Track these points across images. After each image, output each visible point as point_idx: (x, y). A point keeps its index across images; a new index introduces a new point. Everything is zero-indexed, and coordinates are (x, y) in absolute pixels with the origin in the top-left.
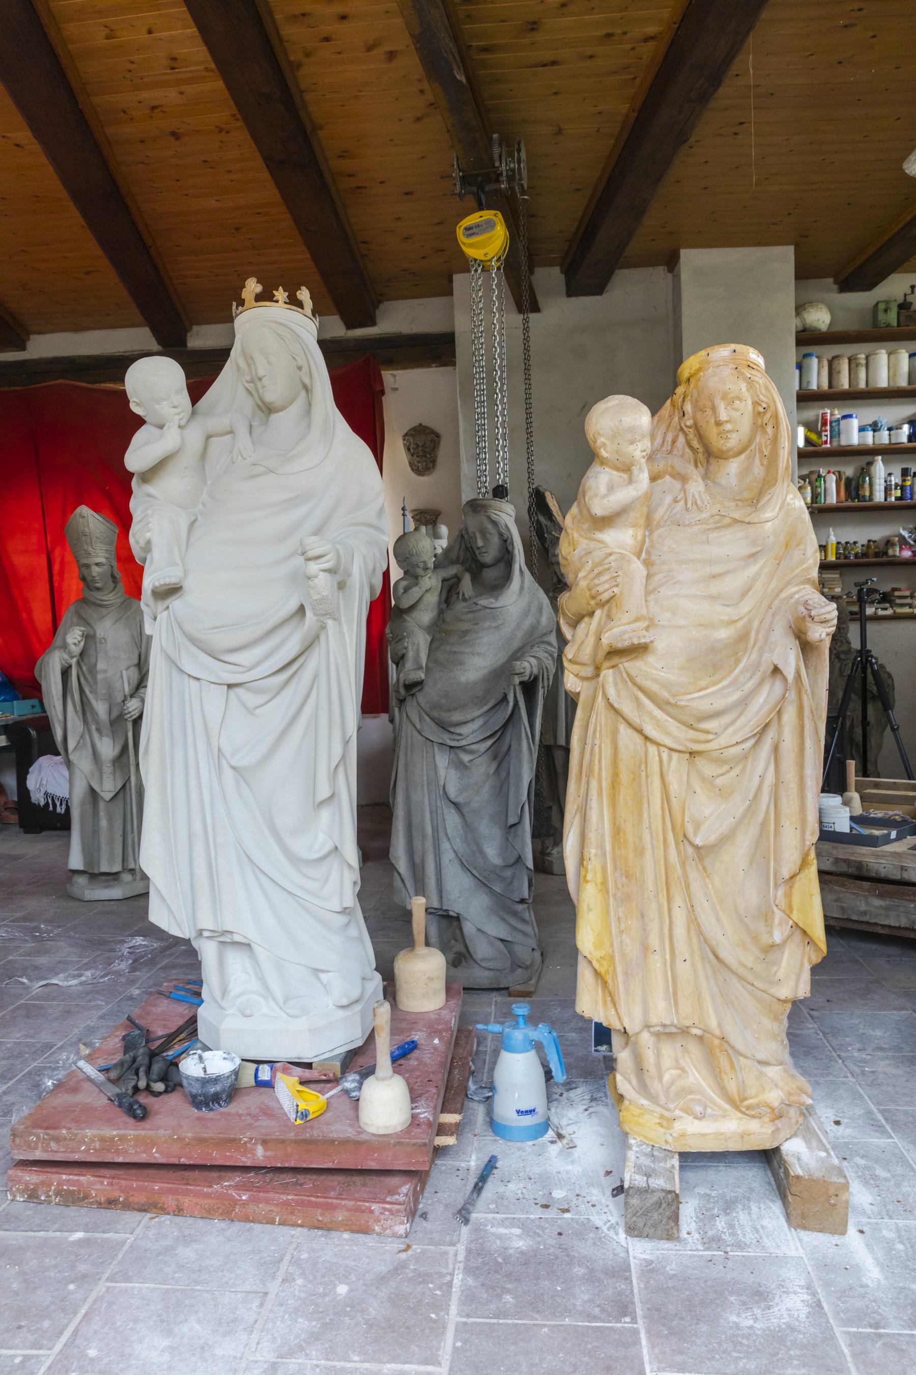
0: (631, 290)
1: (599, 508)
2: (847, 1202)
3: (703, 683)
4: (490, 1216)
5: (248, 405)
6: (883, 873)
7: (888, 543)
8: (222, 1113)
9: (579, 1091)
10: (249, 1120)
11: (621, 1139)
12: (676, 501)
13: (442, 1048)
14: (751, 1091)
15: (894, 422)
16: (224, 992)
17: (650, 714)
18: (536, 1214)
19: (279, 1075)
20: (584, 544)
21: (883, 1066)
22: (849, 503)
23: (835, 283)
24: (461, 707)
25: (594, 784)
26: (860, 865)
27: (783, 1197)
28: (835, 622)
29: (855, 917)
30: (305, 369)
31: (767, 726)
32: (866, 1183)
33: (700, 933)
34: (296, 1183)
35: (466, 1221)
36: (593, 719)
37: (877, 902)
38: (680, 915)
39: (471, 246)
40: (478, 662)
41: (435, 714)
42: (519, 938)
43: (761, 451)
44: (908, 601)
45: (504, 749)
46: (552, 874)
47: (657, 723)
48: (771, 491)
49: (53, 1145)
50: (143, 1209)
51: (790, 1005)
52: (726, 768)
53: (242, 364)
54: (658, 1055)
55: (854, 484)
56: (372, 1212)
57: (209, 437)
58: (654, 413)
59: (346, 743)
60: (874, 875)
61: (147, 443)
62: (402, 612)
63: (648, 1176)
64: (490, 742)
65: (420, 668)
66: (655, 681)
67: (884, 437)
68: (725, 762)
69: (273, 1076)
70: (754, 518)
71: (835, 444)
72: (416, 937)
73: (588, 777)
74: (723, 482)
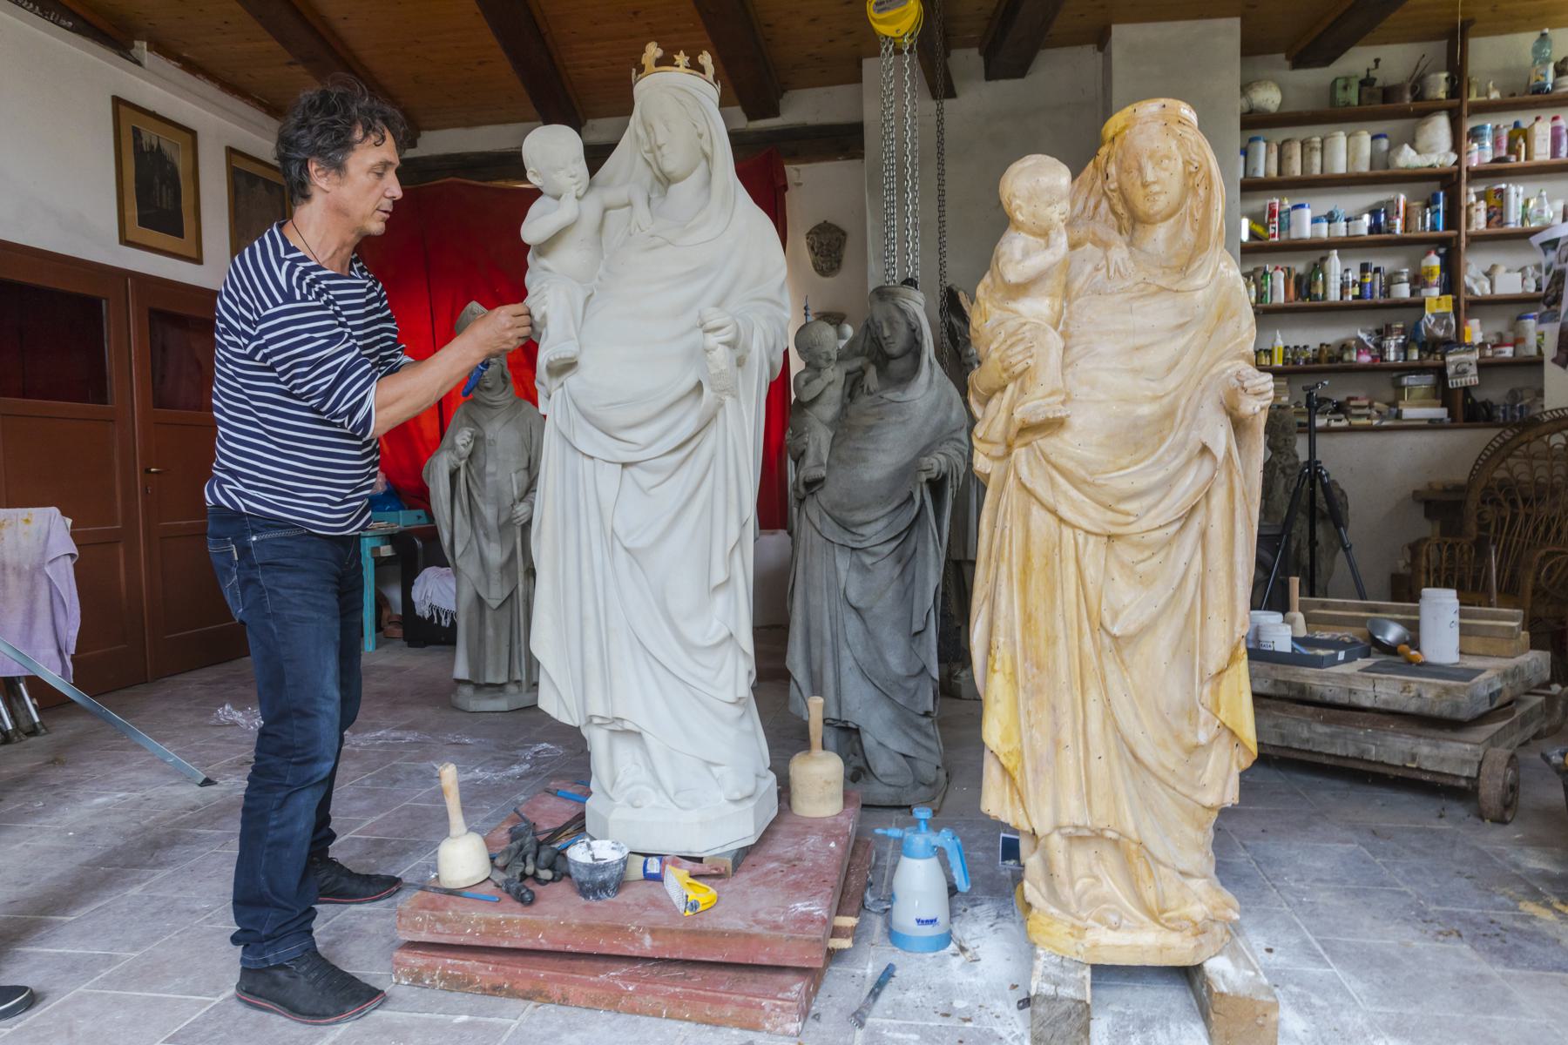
0: (1058, 72)
1: (1013, 274)
2: (1277, 1023)
3: (1124, 462)
4: (887, 1021)
5: (647, 177)
6: (1329, 696)
7: (1344, 347)
8: (610, 903)
9: (984, 907)
10: (637, 910)
11: (1029, 950)
12: (1097, 269)
13: (839, 851)
14: (1172, 904)
15: (1352, 212)
16: (613, 783)
17: (1065, 494)
18: (936, 1021)
19: (668, 867)
20: (996, 315)
21: (1324, 897)
22: (1300, 303)
23: (1287, 58)
24: (865, 507)
25: (1004, 569)
26: (1302, 688)
27: (1205, 1017)
28: (1271, 394)
29: (1296, 745)
30: (706, 136)
31: (1194, 508)
32: (1300, 1010)
33: (1117, 729)
34: (684, 977)
35: (861, 1025)
36: (1004, 500)
37: (1321, 729)
38: (1095, 710)
39: (883, 22)
40: (884, 457)
41: (837, 513)
42: (923, 754)
43: (1192, 215)
44: (1366, 411)
45: (909, 552)
46: (960, 698)
47: (1072, 503)
48: (1203, 256)
49: (439, 926)
50: (527, 997)
51: (1215, 815)
52: (1147, 553)
53: (641, 132)
54: (1070, 860)
55: (1305, 282)
56: (762, 1008)
57: (606, 210)
58: (1075, 175)
59: (743, 525)
60: (1317, 698)
61: (544, 214)
62: (802, 406)
63: (1057, 985)
64: (894, 544)
65: (822, 464)
66: (1072, 459)
67: (1341, 229)
68: (1147, 547)
69: (663, 869)
70: (1183, 286)
71: (1284, 237)
72: (812, 739)
73: (997, 561)
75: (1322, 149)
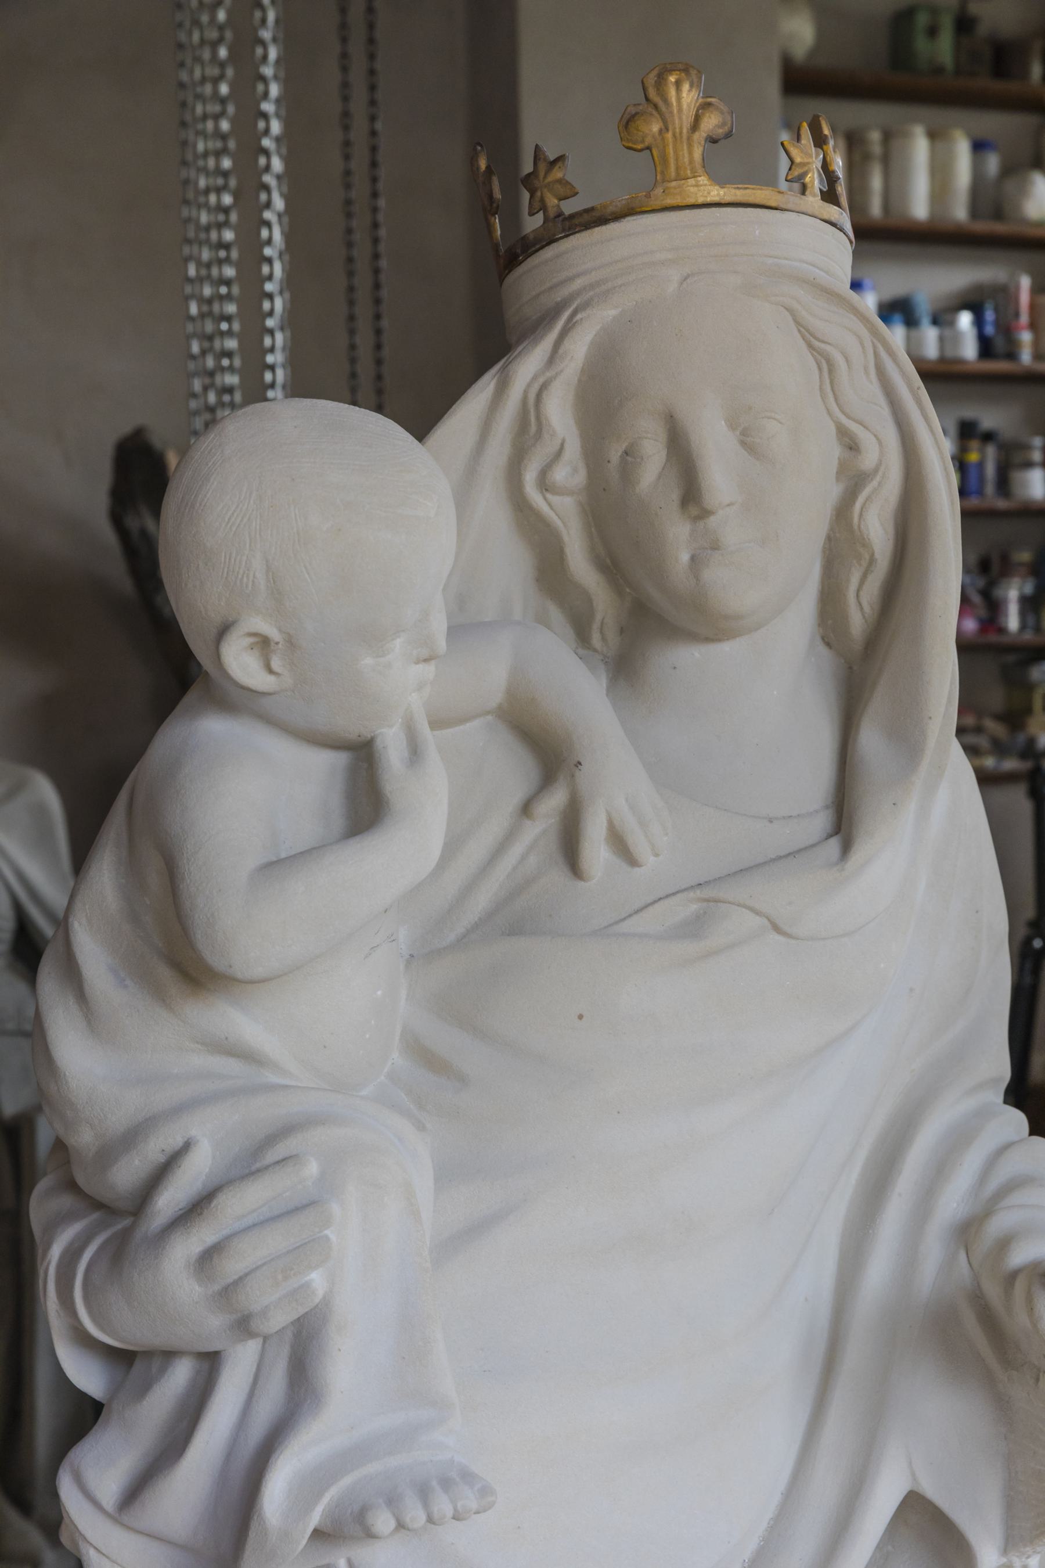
53: (560, 414)
75: (886, 160)
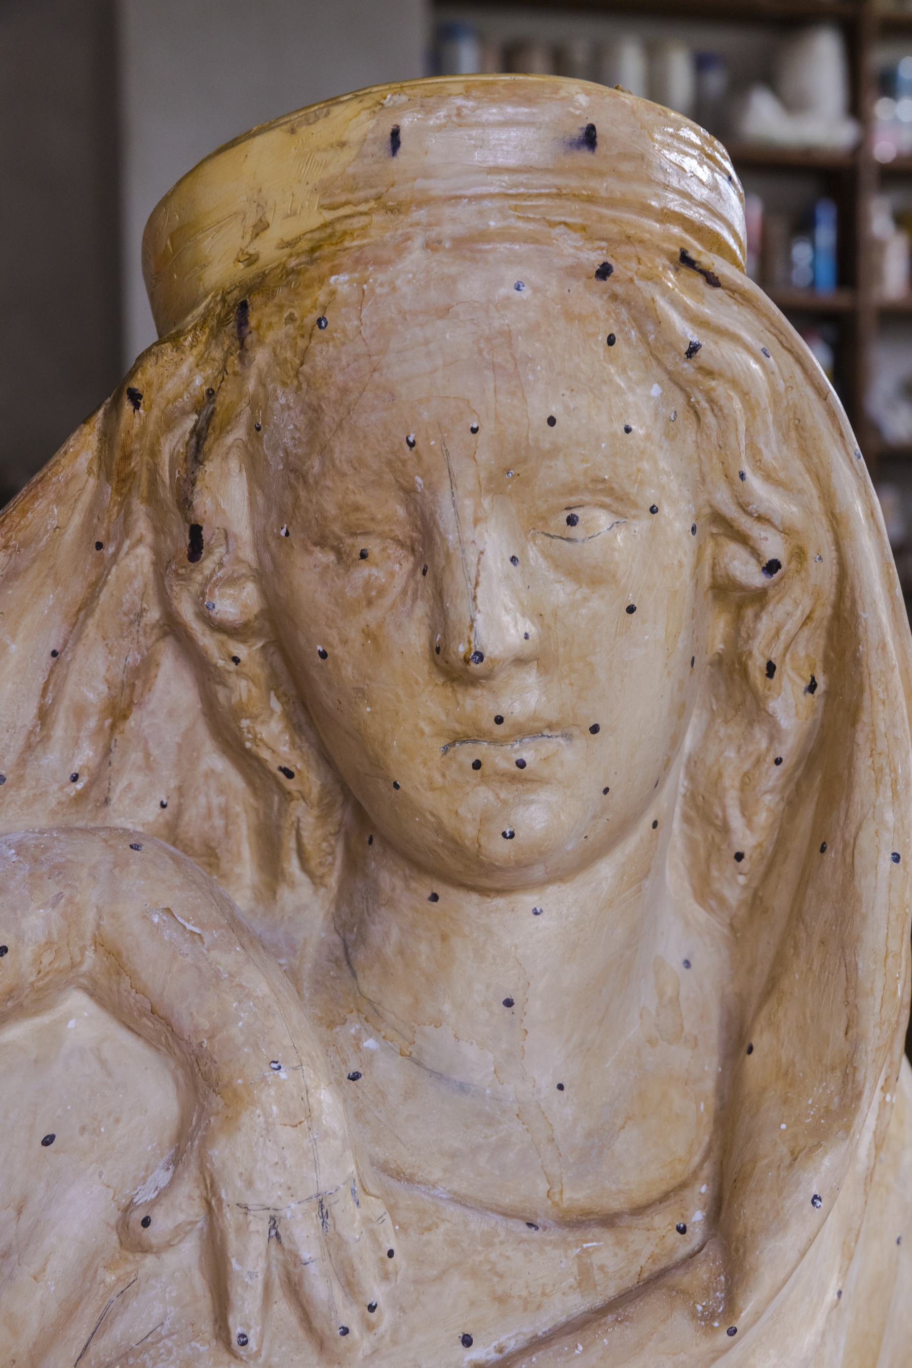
48: (820, 1173)
74: (476, 1061)
